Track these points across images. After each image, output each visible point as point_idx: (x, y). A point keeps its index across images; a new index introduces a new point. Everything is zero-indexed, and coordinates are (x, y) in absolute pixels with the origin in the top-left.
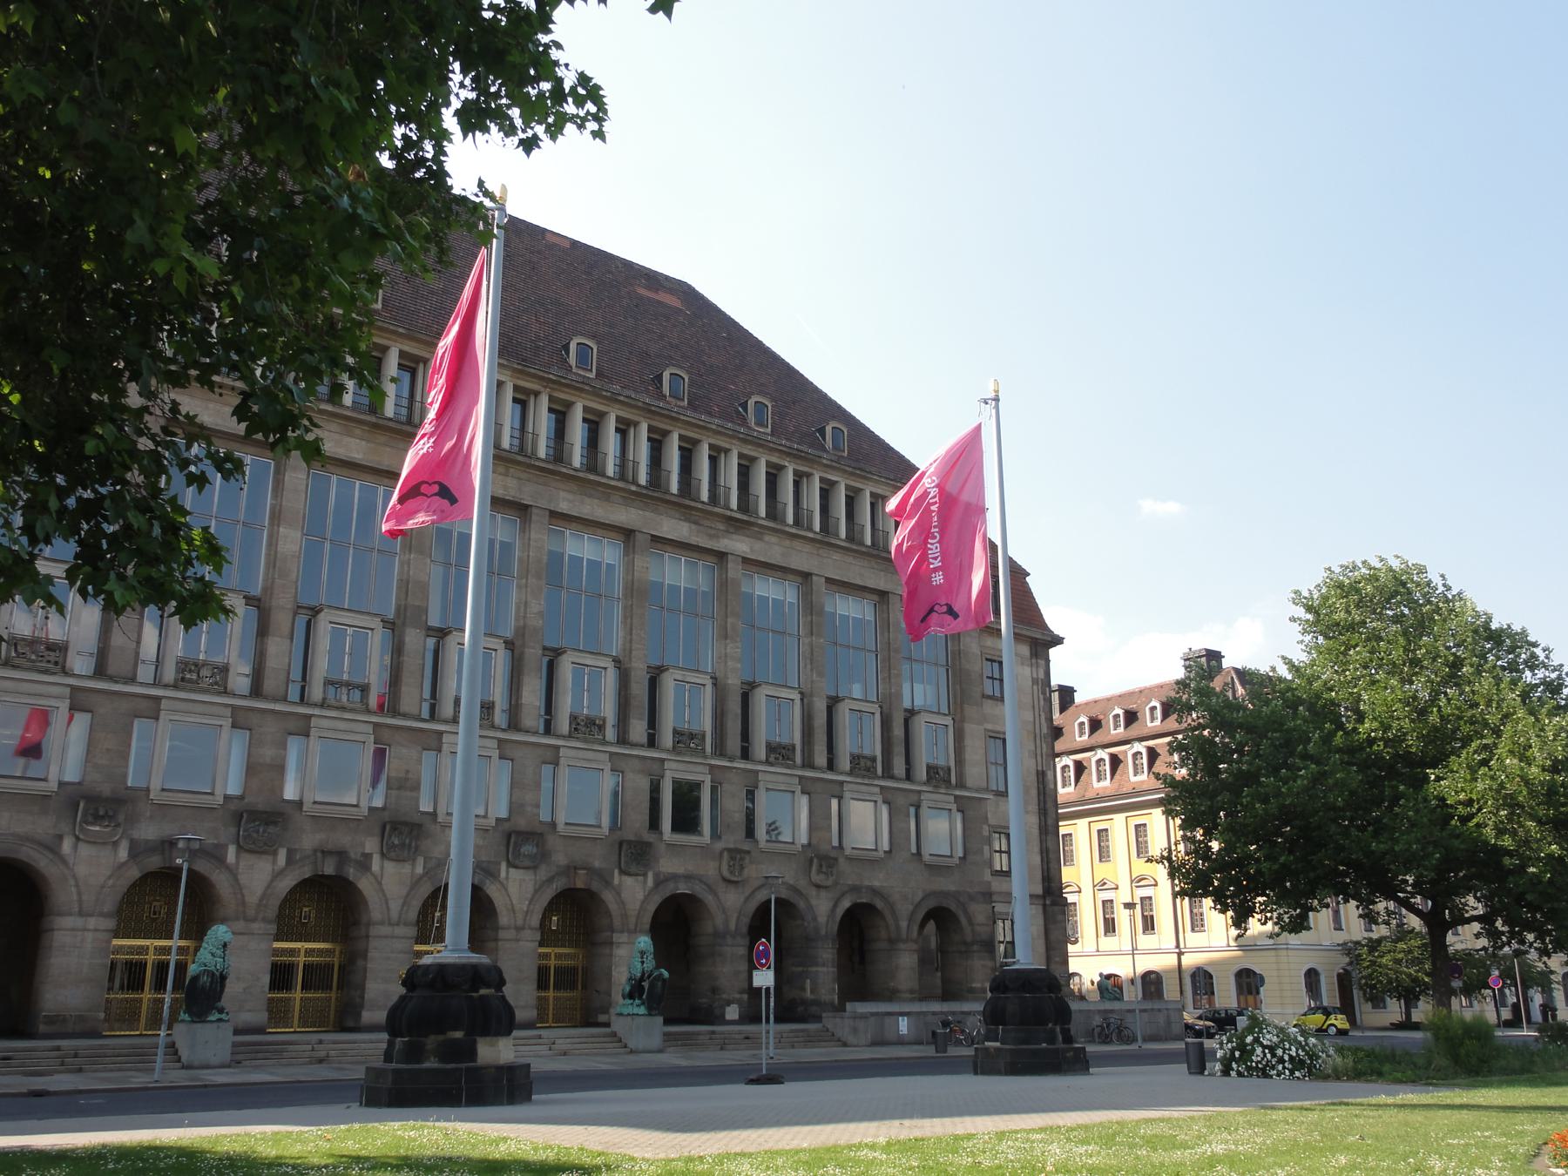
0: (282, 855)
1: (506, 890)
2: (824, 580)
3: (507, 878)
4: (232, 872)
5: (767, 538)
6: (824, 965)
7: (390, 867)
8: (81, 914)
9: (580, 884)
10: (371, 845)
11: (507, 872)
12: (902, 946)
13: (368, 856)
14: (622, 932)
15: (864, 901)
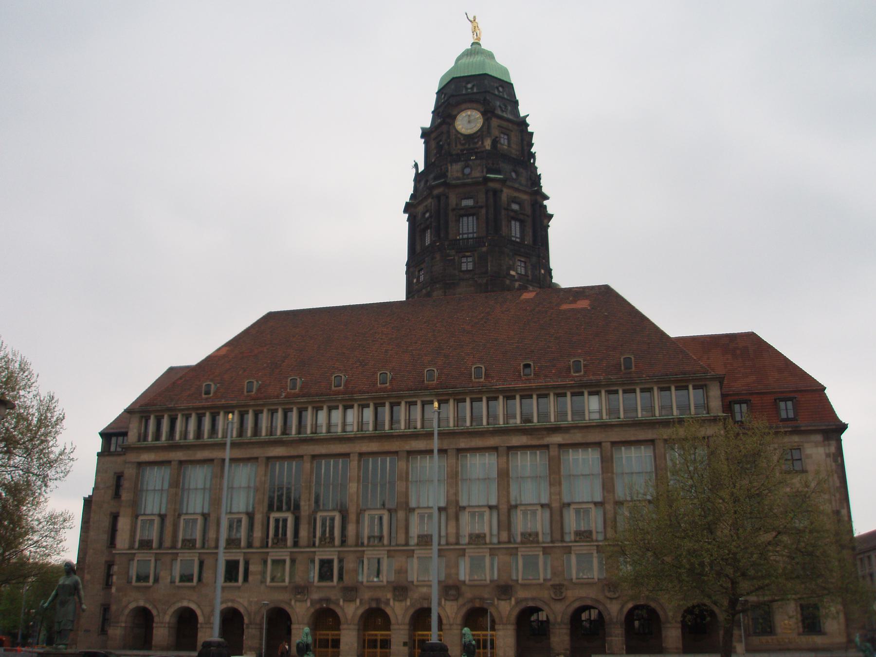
0: (358, 601)
1: (445, 609)
2: (609, 444)
3: (445, 605)
4: (342, 608)
5: (572, 431)
6: (616, 636)
7: (397, 604)
8: (298, 624)
9: (477, 605)
10: (389, 596)
11: (445, 602)
12: (669, 625)
13: (389, 600)
14: (500, 624)
15: (642, 603)
